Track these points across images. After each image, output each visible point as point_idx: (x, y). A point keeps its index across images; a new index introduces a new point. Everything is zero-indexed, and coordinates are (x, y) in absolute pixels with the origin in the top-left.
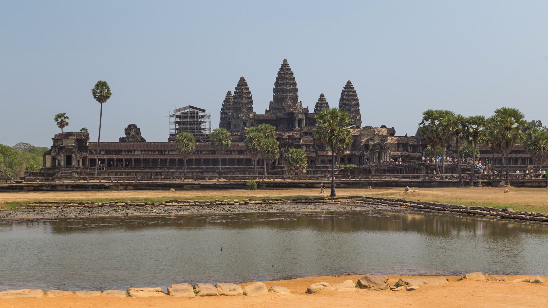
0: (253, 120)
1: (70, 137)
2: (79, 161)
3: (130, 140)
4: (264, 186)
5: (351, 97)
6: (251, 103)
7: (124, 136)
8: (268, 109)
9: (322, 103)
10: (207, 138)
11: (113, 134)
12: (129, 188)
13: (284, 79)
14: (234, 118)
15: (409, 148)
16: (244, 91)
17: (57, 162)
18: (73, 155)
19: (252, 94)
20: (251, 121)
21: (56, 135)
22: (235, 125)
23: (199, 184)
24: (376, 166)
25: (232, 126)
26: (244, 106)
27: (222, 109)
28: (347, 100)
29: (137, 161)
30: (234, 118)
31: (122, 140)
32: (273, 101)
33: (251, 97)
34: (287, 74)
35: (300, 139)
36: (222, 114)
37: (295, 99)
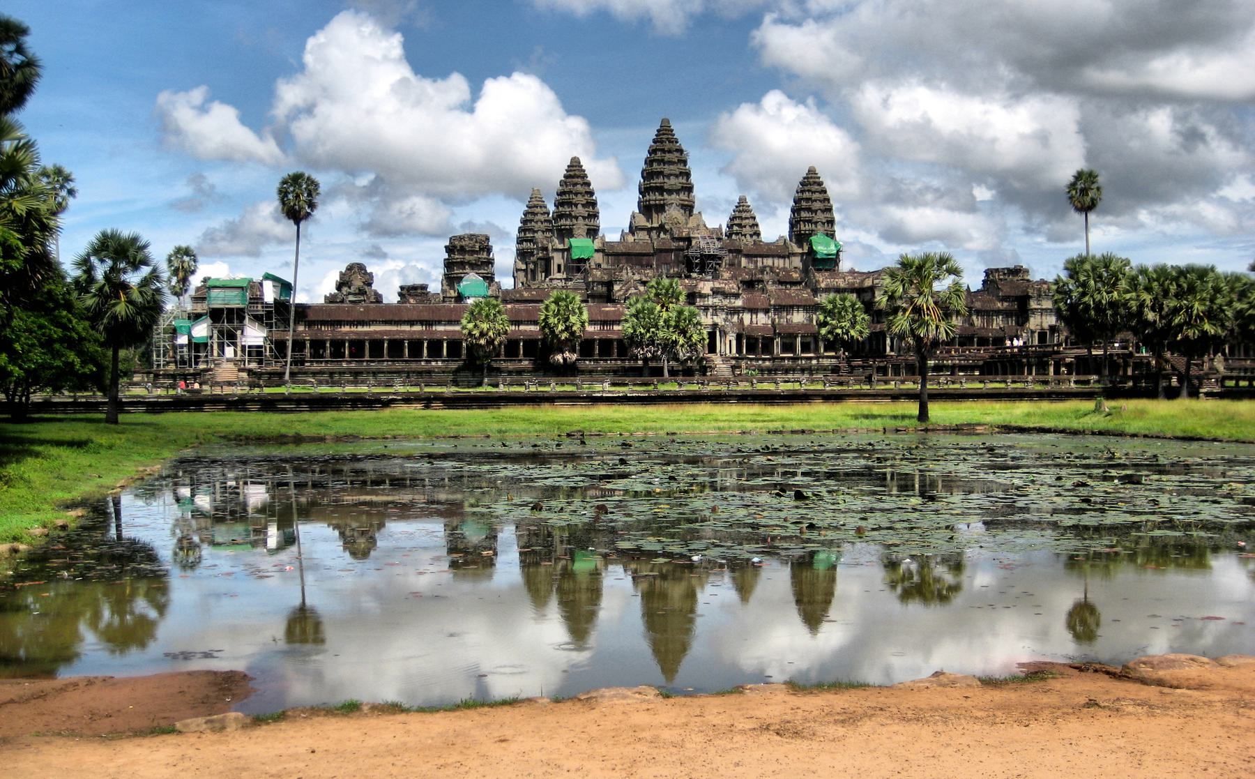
0: (601, 254)
8: (627, 231)
9: (742, 218)
10: (507, 297)
11: (316, 287)
16: (579, 188)
19: (598, 197)
22: (559, 266)
25: (554, 268)
27: (521, 230)
28: (809, 210)
29: (376, 346)
31: (331, 299)
32: (637, 211)
33: (594, 204)
34: (670, 151)
35: (737, 296)
36: (520, 241)
37: (688, 208)
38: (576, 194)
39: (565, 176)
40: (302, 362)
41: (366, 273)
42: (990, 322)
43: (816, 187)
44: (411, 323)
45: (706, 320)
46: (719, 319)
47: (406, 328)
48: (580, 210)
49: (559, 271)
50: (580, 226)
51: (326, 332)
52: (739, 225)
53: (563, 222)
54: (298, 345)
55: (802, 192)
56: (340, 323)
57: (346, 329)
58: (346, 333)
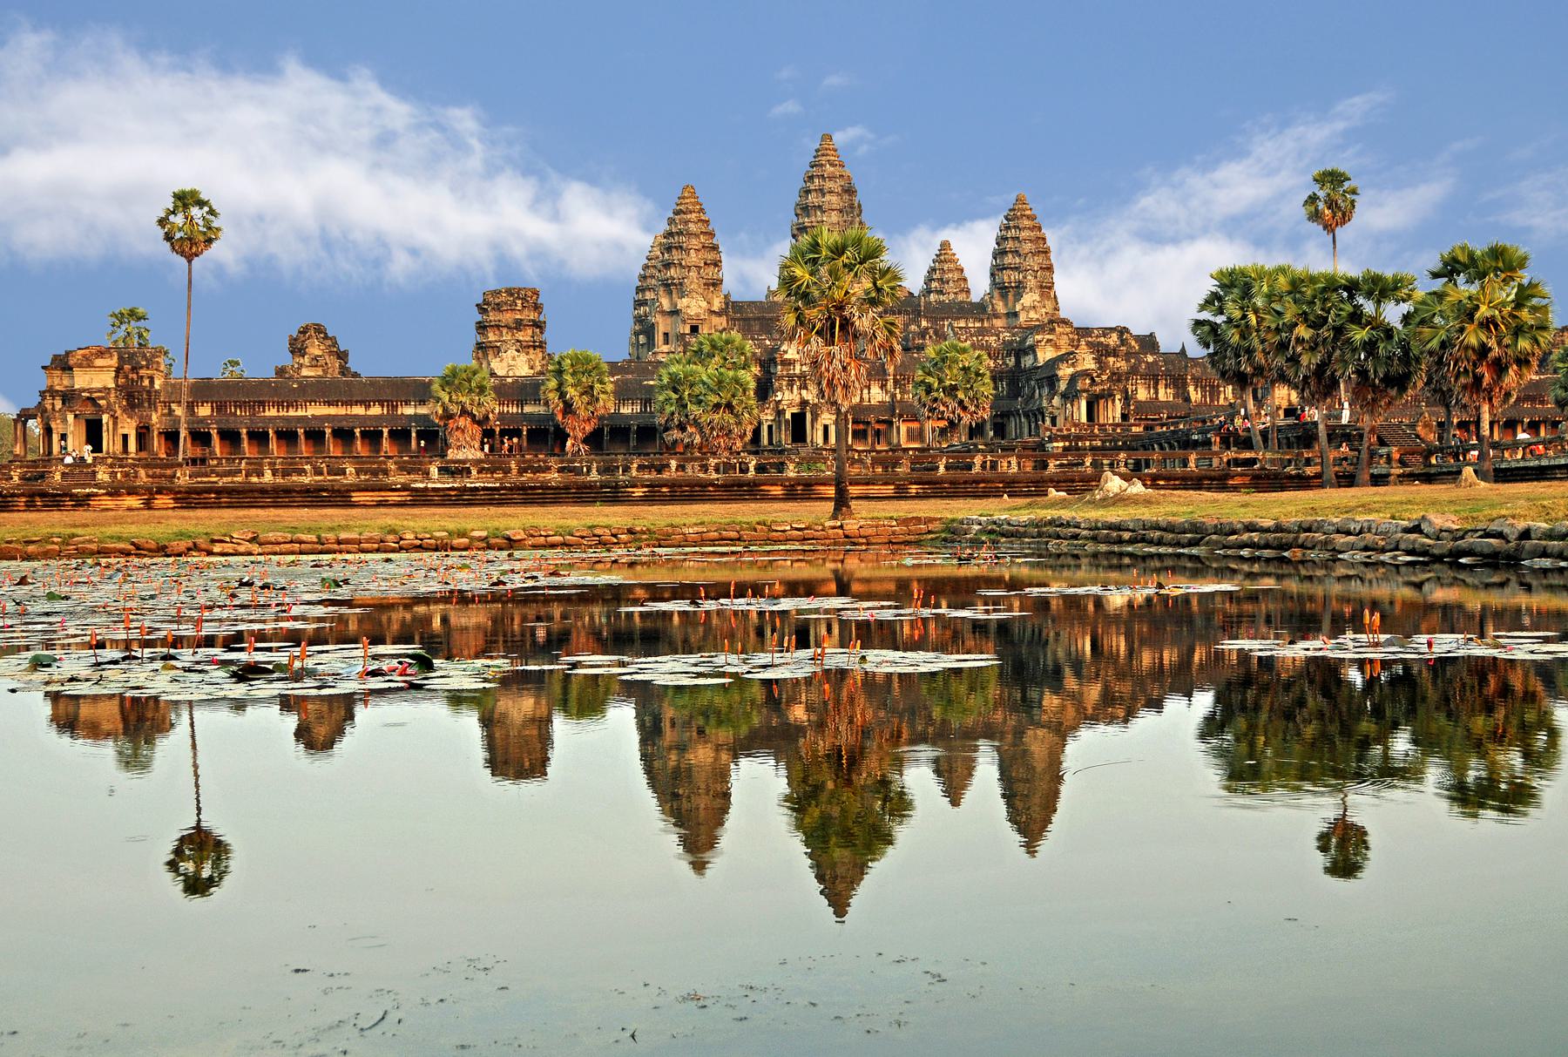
1: (99, 362)
2: (125, 437)
3: (305, 372)
4: (639, 492)
5: (1028, 247)
6: (716, 264)
7: (286, 359)
12: (163, 501)
13: (822, 192)
14: (663, 312)
15: (1191, 389)
17: (55, 438)
18: (105, 418)
20: (716, 320)
21: (56, 358)
22: (666, 334)
23: (405, 488)
24: (1064, 438)
25: (659, 338)
26: (693, 274)
28: (1016, 253)
29: (315, 436)
30: (663, 312)
31: (281, 372)
36: (639, 304)
38: (690, 234)
39: (677, 213)
40: (203, 461)
41: (326, 337)
42: (1215, 392)
43: (1026, 223)
44: (366, 404)
45: (788, 398)
46: (810, 395)
47: (359, 410)
48: (693, 258)
49: (666, 342)
50: (693, 280)
51: (241, 419)
52: (941, 280)
53: (672, 272)
54: (200, 437)
55: (1008, 228)
56: (262, 404)
57: (273, 412)
58: (272, 419)
